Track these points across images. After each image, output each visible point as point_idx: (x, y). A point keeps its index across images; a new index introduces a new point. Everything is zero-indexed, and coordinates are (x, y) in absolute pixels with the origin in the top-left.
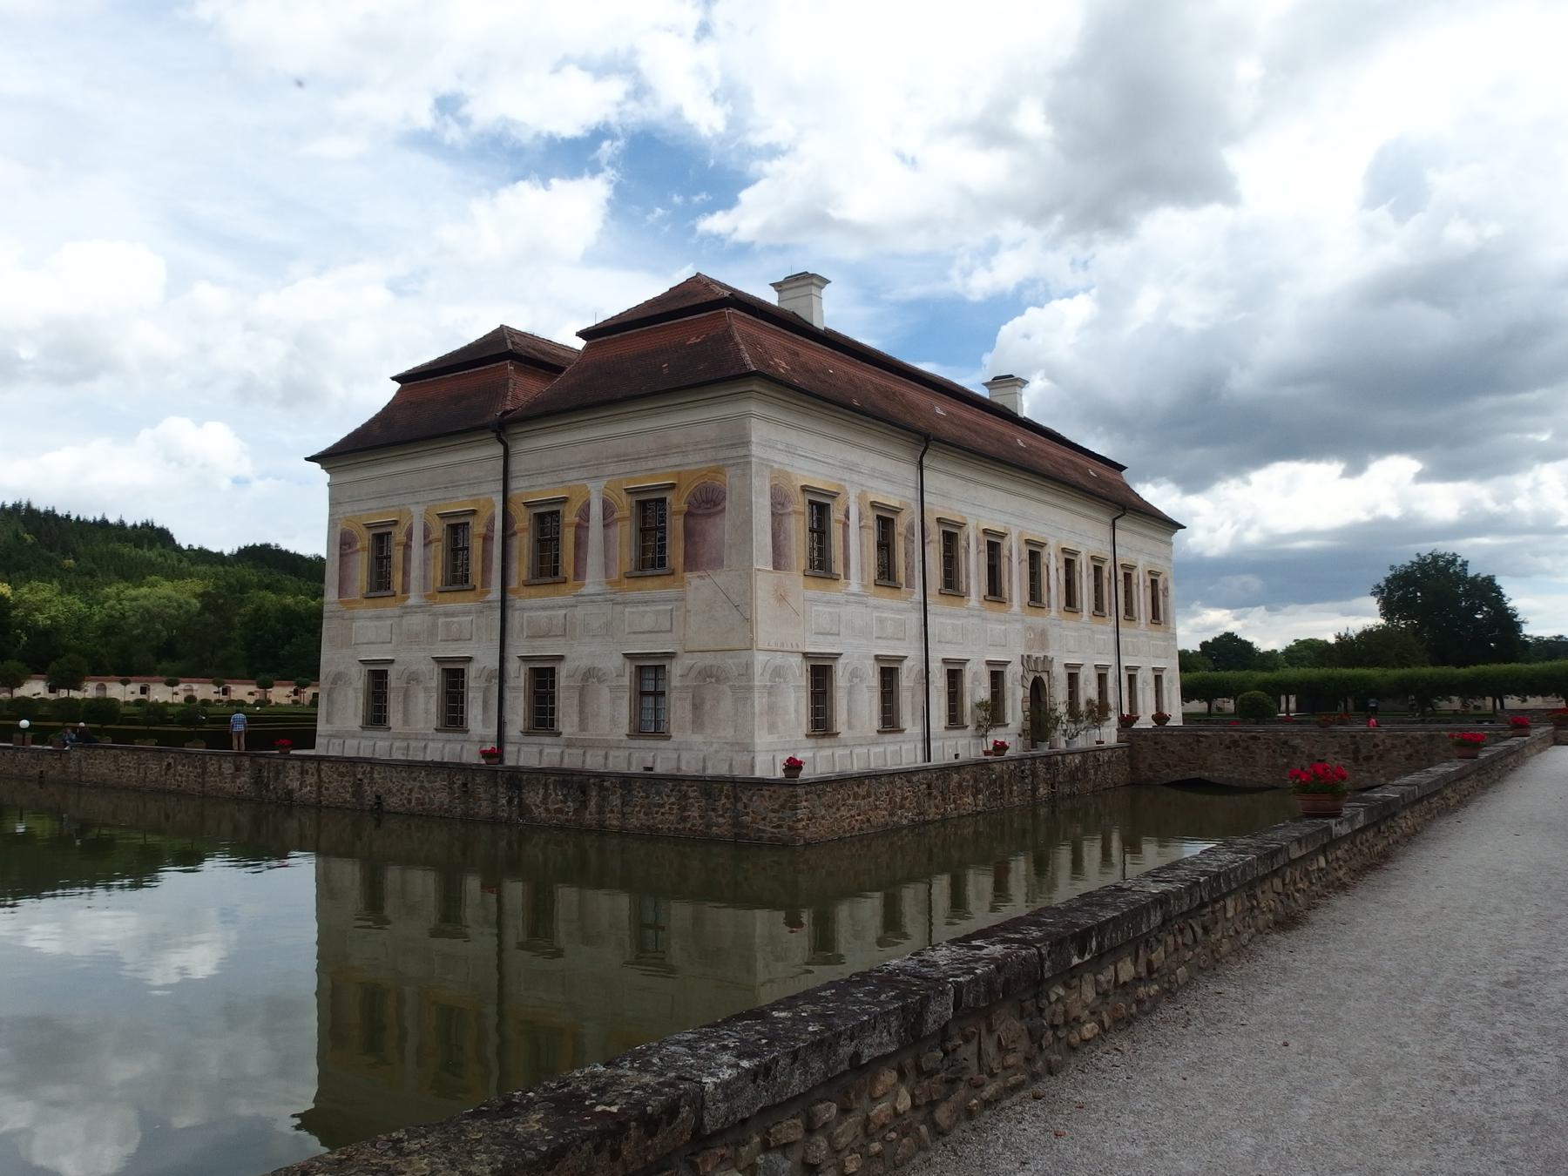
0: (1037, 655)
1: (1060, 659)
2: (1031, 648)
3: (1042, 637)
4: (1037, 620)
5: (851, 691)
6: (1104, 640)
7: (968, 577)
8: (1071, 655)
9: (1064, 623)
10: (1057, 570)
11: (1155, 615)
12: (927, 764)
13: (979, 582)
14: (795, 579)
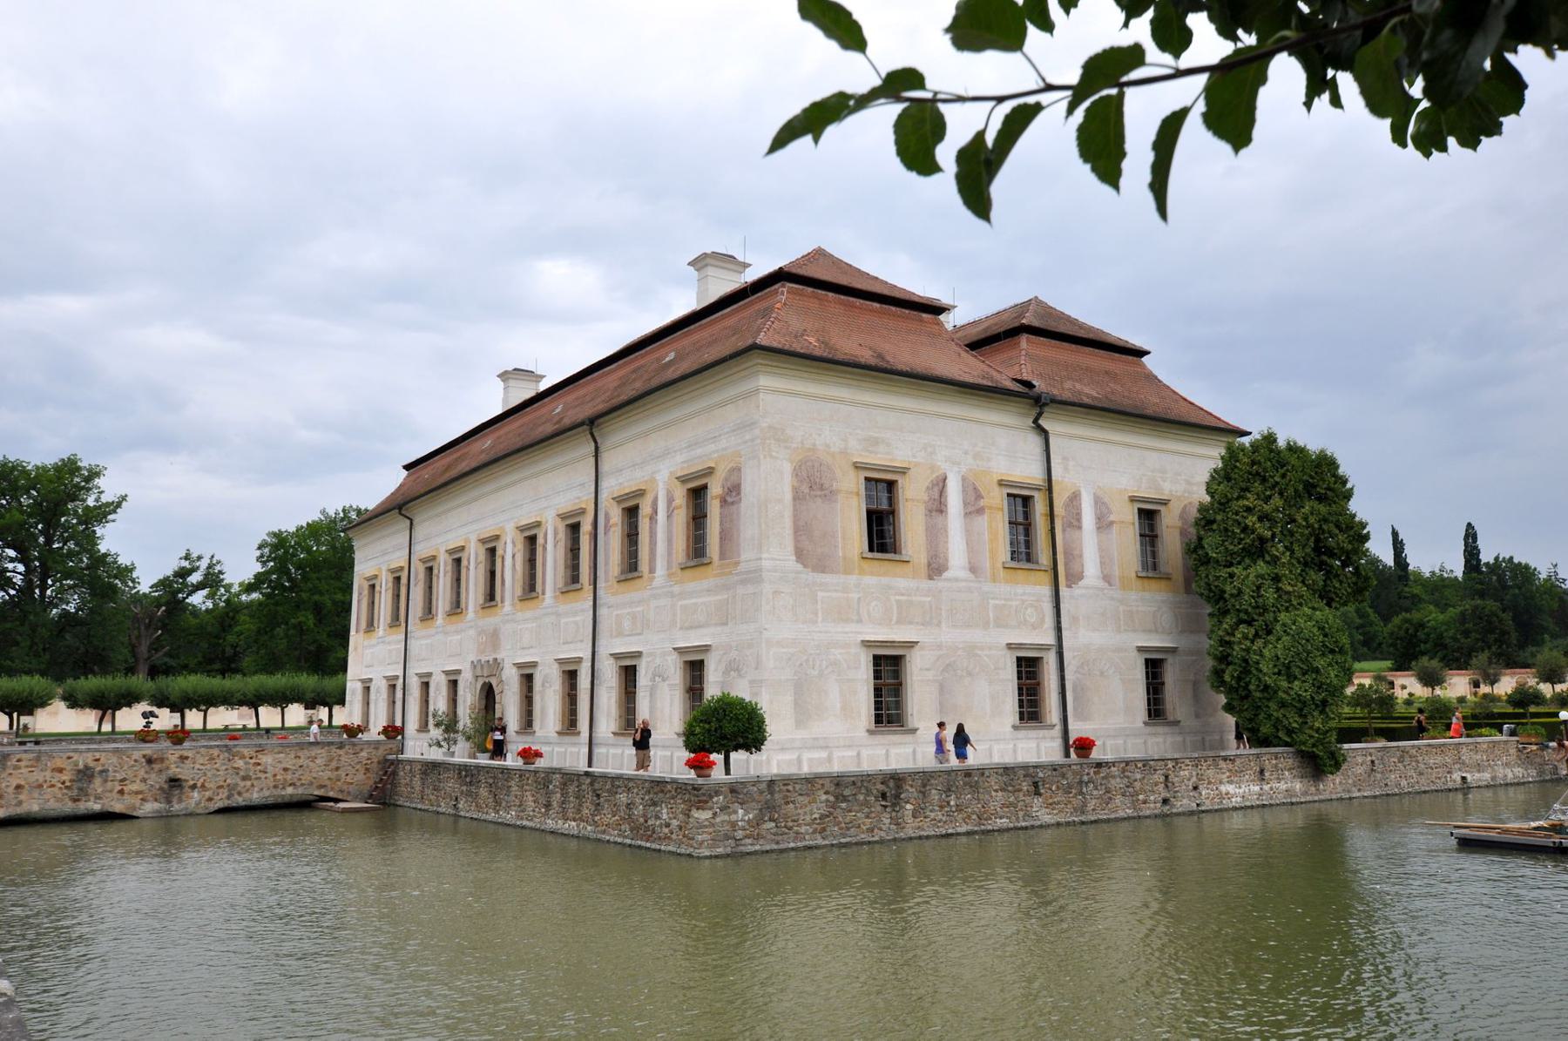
0: (487, 658)
1: (511, 657)
2: (483, 652)
3: (494, 638)
4: (491, 620)
5: (376, 700)
6: (576, 623)
7: (437, 599)
8: (527, 652)
9: (520, 615)
10: (514, 556)
11: (697, 550)
12: (483, 760)
13: (444, 600)
14: (361, 633)
